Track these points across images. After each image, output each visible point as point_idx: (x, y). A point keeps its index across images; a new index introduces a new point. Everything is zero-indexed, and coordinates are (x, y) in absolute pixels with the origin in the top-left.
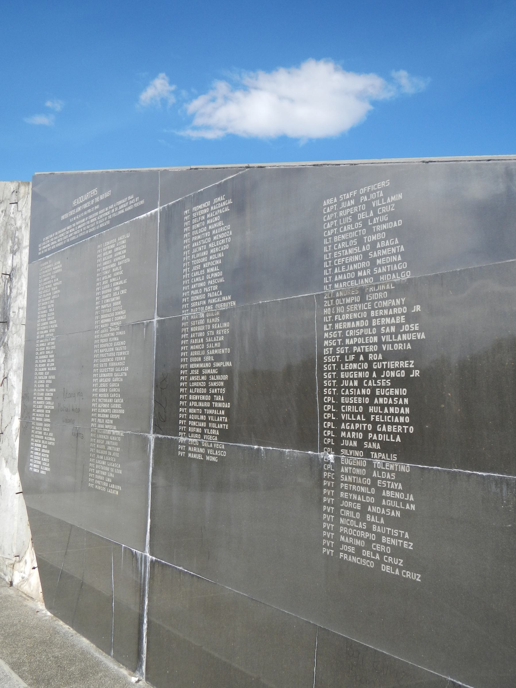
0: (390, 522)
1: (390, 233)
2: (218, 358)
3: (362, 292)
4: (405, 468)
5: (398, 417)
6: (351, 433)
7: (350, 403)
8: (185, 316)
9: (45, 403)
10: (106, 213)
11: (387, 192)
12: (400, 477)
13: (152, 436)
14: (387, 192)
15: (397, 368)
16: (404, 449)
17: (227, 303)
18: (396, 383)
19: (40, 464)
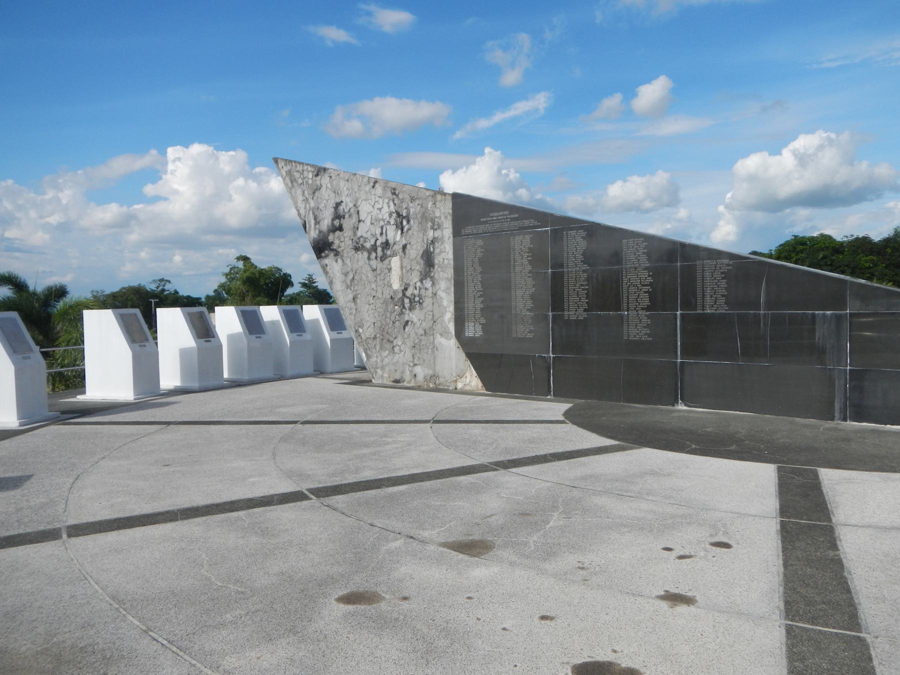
0: (644, 327)
1: (644, 253)
2: (582, 285)
3: (636, 268)
4: (648, 313)
5: (646, 302)
6: (632, 306)
7: (632, 298)
8: (565, 270)
9: (474, 304)
10: (516, 223)
11: (643, 242)
12: (646, 316)
13: (550, 314)
14: (643, 242)
15: (646, 289)
16: (648, 309)
17: (585, 267)
18: (645, 292)
19: (473, 330)
